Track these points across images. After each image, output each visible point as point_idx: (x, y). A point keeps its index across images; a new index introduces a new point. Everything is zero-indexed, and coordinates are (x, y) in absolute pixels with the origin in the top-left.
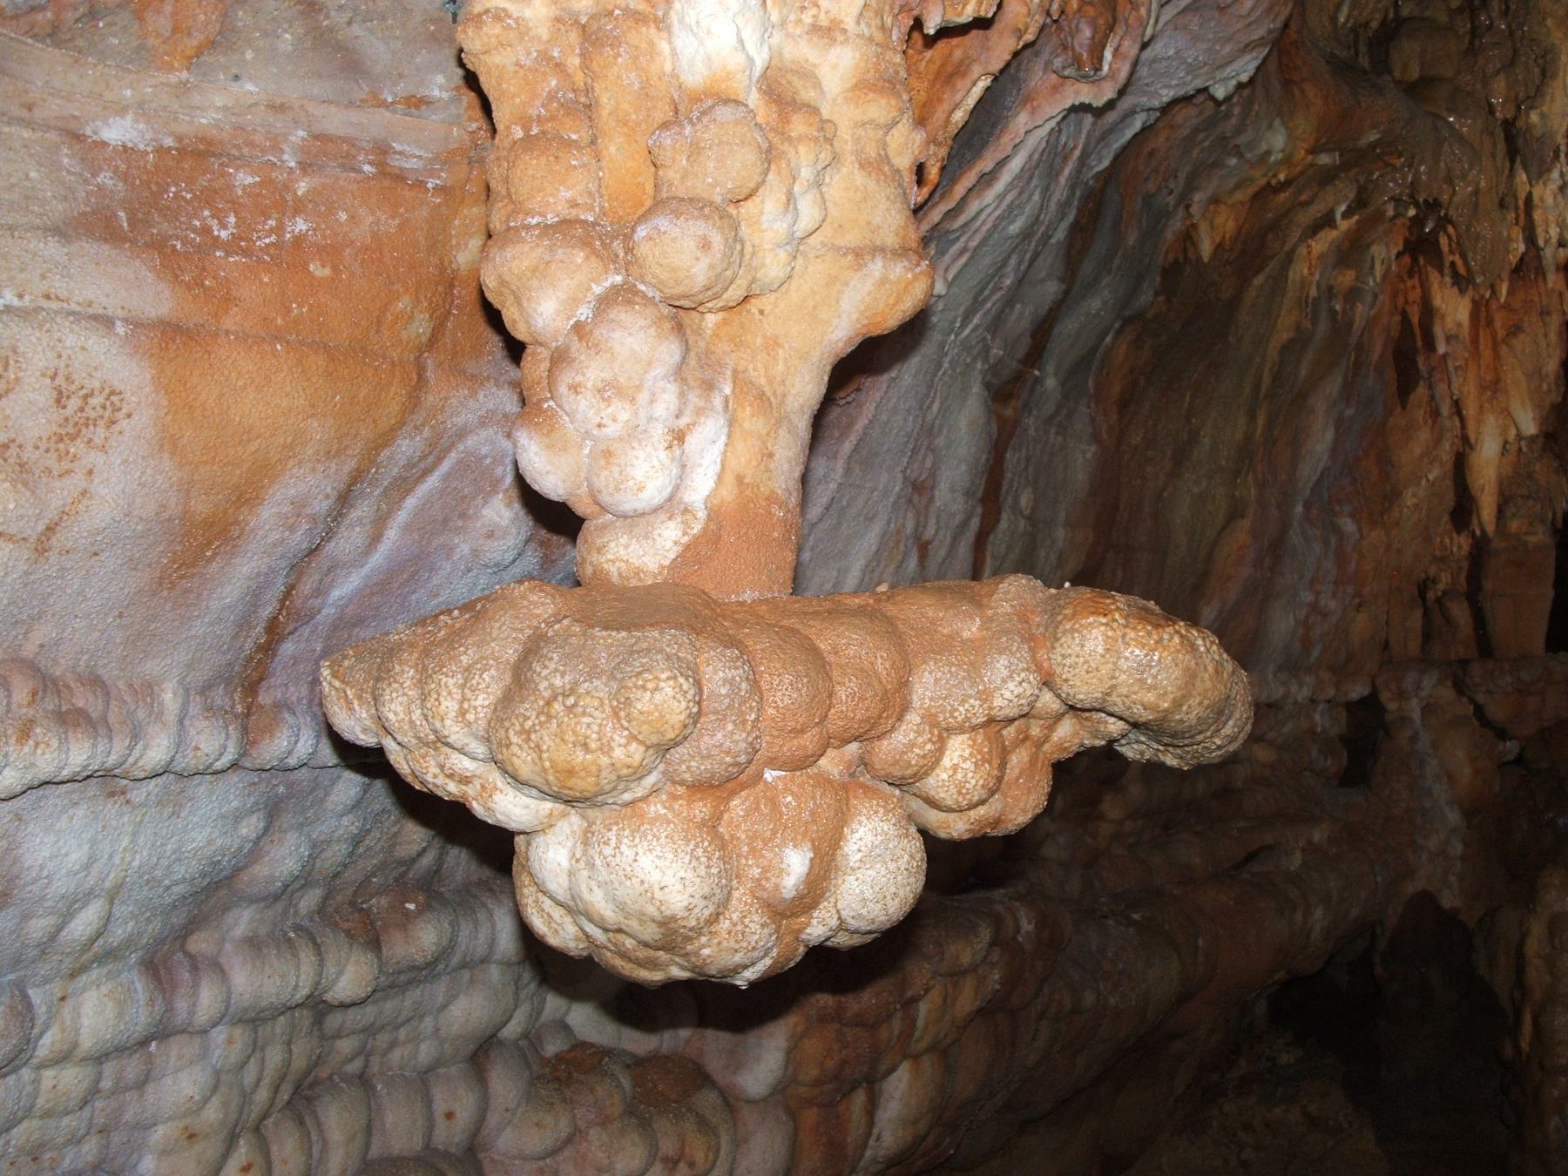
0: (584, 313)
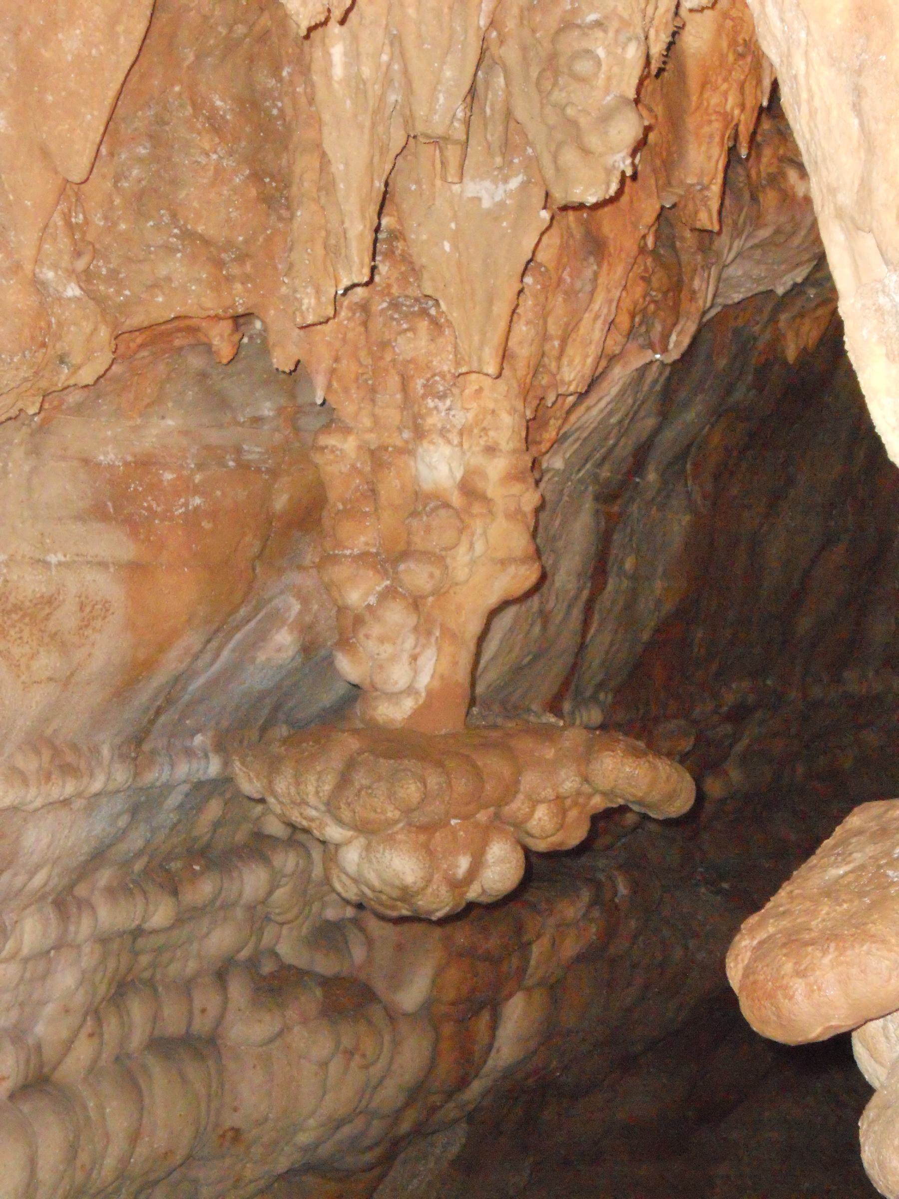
0: (372, 600)
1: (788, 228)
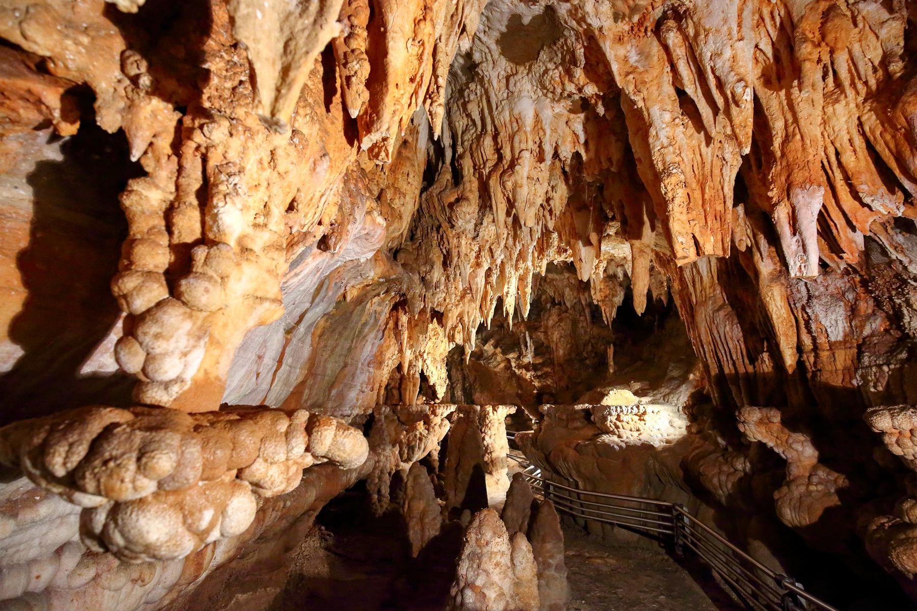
1: (372, 233)
